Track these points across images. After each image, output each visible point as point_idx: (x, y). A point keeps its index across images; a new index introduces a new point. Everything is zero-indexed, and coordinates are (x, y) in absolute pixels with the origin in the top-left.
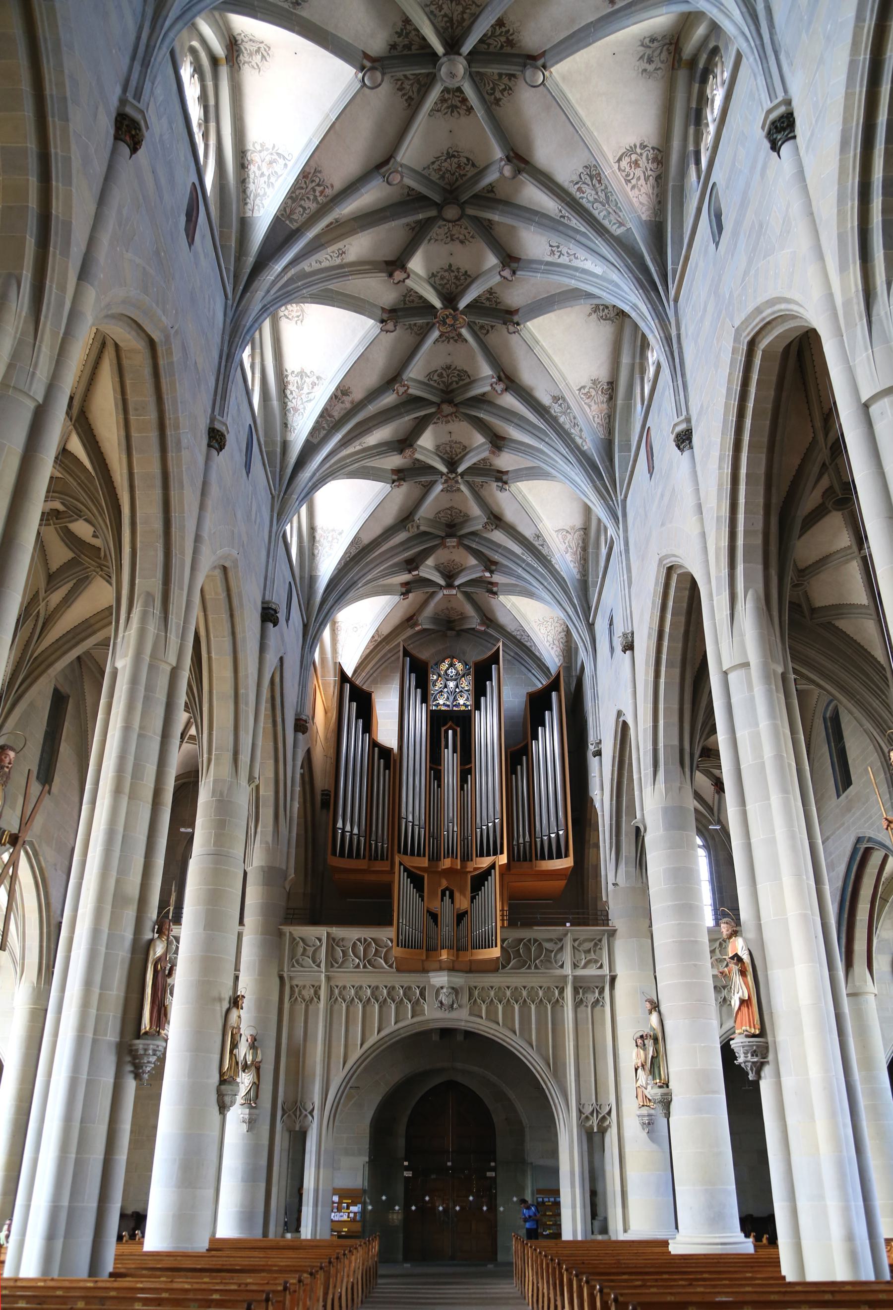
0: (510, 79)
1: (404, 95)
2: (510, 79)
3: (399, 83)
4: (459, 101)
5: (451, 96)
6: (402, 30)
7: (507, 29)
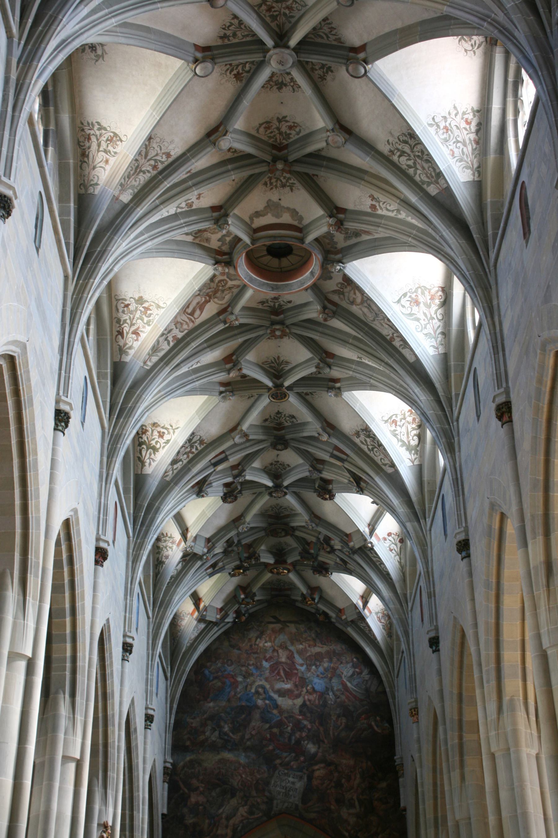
0: (225, 34)
1: (330, 24)
2: (225, 34)
3: (333, 33)
4: (274, 7)
5: (283, 10)
6: (327, 73)
7: (233, 73)
